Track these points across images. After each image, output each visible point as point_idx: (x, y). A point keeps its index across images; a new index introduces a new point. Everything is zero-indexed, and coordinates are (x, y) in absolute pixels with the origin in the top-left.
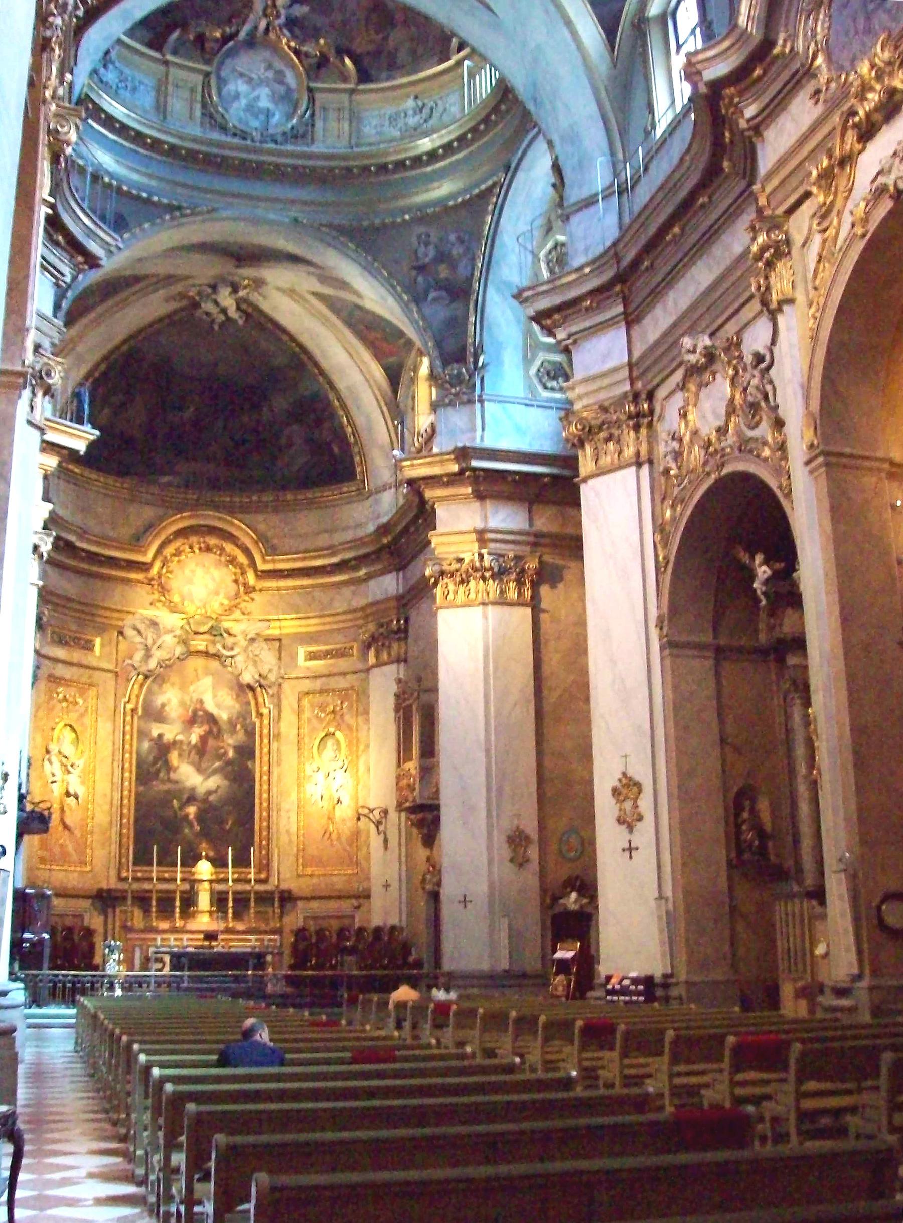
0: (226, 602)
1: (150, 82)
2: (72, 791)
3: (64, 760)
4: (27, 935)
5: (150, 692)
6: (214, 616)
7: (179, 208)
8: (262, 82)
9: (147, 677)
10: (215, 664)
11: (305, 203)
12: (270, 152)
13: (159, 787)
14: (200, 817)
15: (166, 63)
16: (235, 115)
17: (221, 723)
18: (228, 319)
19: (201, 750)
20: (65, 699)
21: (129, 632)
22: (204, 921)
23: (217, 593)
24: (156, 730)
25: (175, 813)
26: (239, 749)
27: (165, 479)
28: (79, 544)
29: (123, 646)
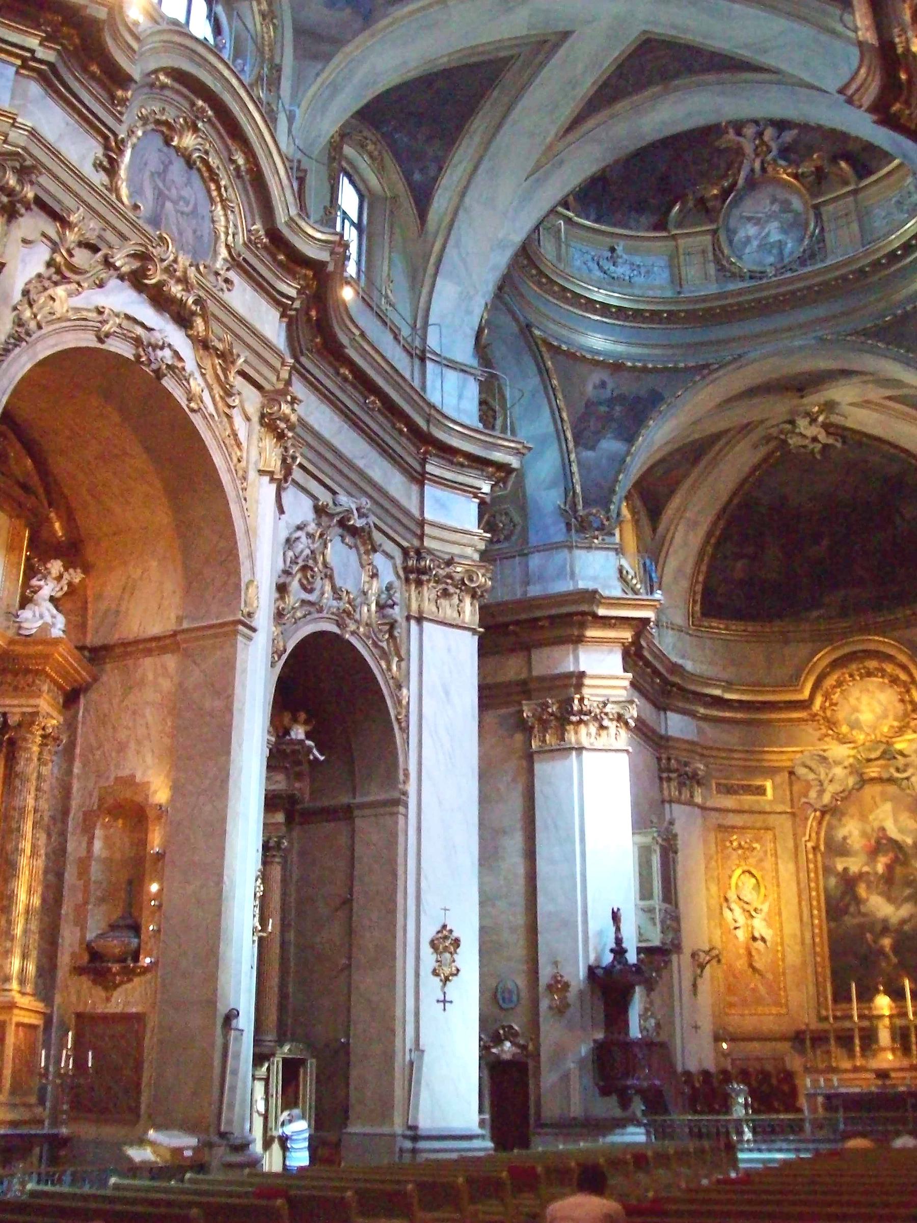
0: (896, 724)
1: (662, 262)
2: (757, 935)
3: (746, 906)
4: (629, 1082)
5: (830, 828)
6: (884, 740)
7: (706, 366)
8: (771, 217)
9: (823, 813)
10: (892, 789)
11: (826, 320)
12: (791, 281)
13: (850, 921)
14: (896, 948)
15: (674, 237)
16: (749, 260)
18: (826, 447)
19: (888, 879)
20: (740, 847)
21: (801, 771)
22: (888, 1059)
23: (885, 716)
27: (815, 614)
28: (728, 696)
29: (796, 788)
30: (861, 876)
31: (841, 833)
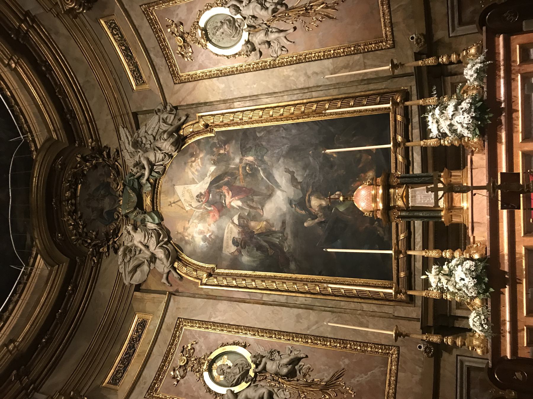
2: (285, 371)
17: (219, 173)
24: (230, 249)
25: (320, 223)
26: (244, 151)
30: (244, 227)
31: (200, 242)
